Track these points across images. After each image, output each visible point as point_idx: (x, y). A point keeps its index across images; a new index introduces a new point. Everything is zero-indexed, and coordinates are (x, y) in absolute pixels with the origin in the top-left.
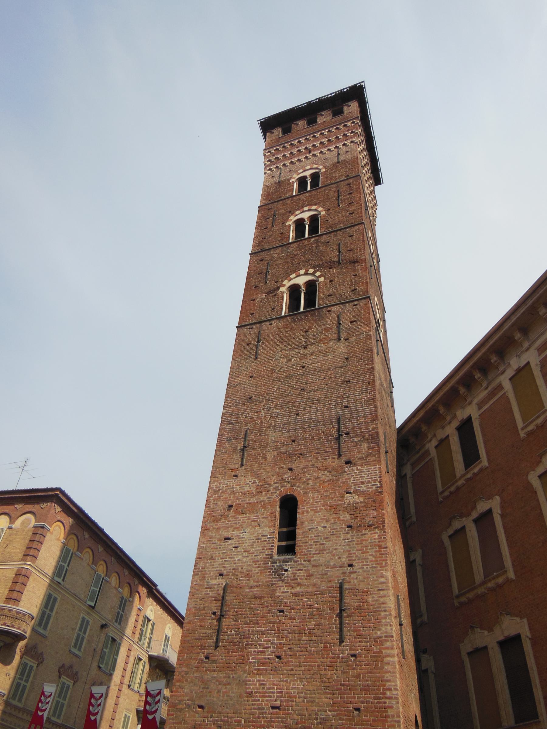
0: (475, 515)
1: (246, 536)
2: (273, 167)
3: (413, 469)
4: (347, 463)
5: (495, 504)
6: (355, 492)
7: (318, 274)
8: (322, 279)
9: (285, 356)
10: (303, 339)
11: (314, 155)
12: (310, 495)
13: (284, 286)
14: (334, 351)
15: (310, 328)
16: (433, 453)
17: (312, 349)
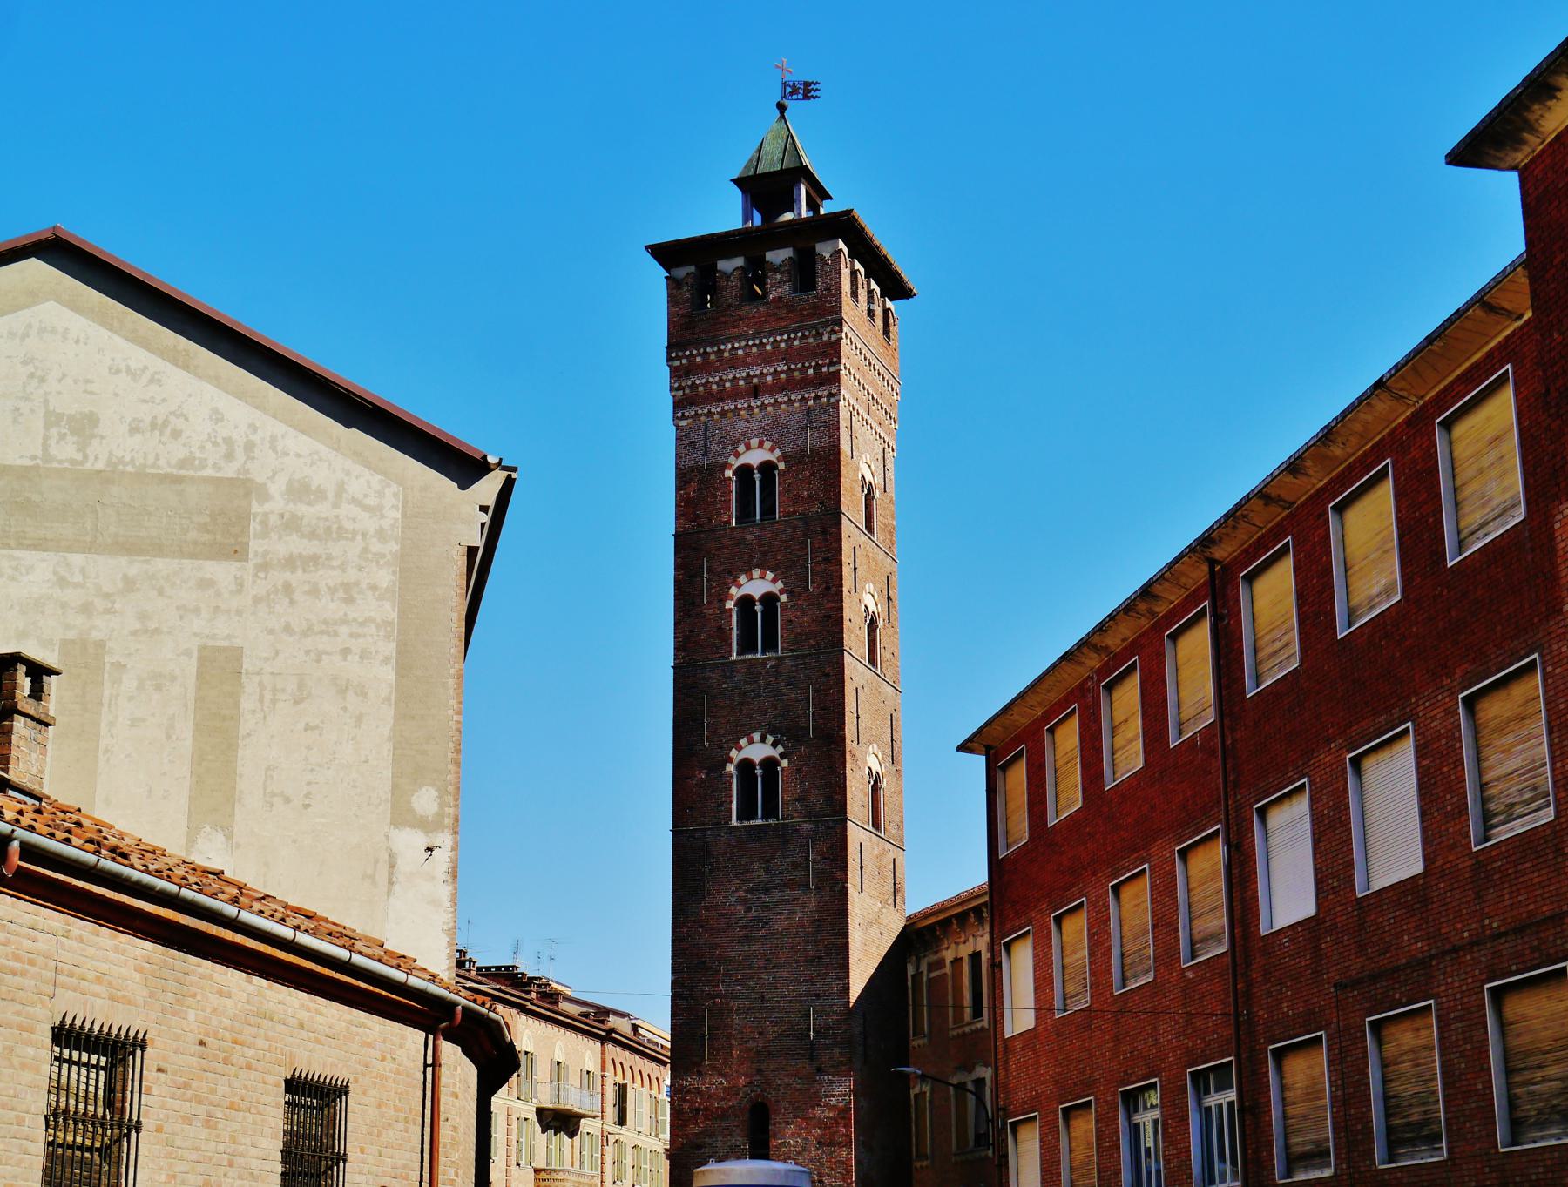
0: (975, 1076)
1: (720, 1144)
2: (690, 412)
3: (929, 971)
4: (820, 1071)
5: (986, 1073)
6: (827, 1105)
7: (780, 749)
8: (785, 763)
9: (743, 901)
10: (764, 877)
11: (763, 407)
12: (782, 1104)
13: (730, 760)
14: (803, 905)
15: (773, 858)
16: (948, 970)
17: (777, 896)
